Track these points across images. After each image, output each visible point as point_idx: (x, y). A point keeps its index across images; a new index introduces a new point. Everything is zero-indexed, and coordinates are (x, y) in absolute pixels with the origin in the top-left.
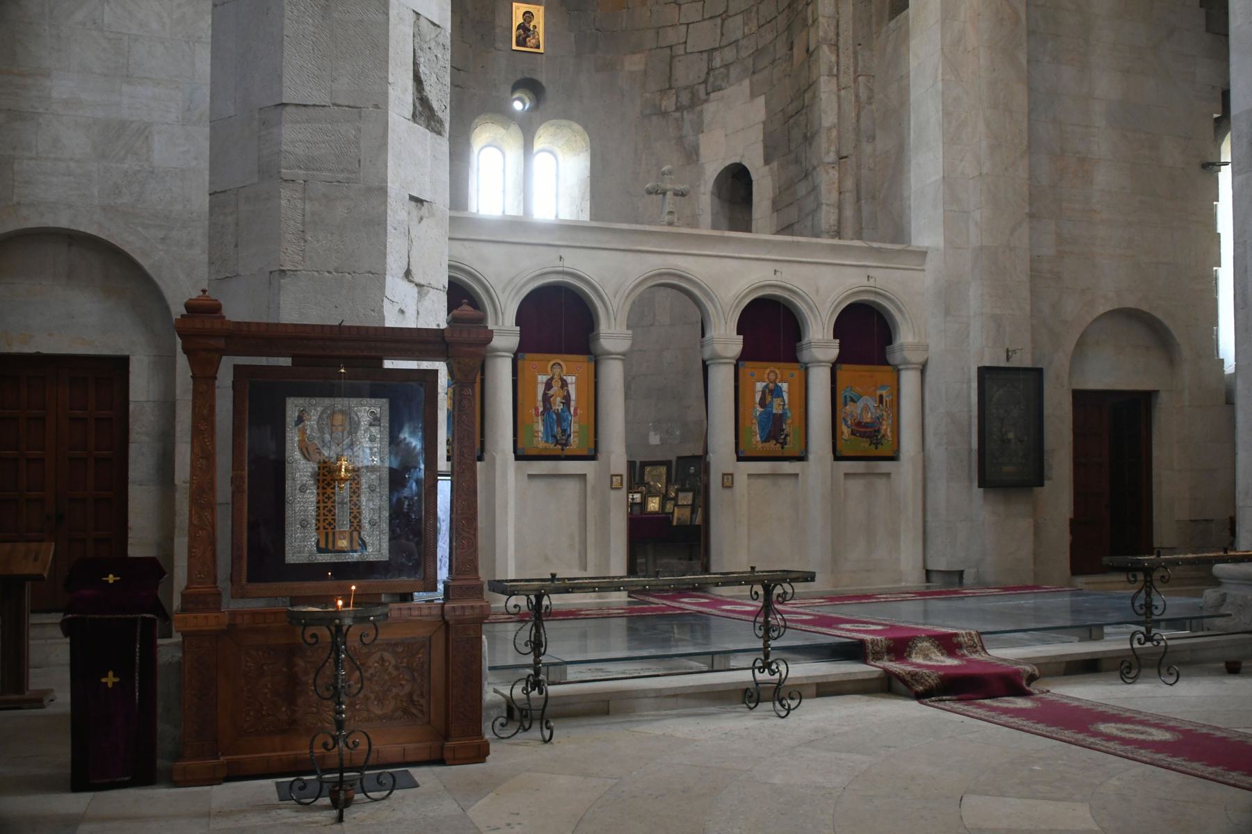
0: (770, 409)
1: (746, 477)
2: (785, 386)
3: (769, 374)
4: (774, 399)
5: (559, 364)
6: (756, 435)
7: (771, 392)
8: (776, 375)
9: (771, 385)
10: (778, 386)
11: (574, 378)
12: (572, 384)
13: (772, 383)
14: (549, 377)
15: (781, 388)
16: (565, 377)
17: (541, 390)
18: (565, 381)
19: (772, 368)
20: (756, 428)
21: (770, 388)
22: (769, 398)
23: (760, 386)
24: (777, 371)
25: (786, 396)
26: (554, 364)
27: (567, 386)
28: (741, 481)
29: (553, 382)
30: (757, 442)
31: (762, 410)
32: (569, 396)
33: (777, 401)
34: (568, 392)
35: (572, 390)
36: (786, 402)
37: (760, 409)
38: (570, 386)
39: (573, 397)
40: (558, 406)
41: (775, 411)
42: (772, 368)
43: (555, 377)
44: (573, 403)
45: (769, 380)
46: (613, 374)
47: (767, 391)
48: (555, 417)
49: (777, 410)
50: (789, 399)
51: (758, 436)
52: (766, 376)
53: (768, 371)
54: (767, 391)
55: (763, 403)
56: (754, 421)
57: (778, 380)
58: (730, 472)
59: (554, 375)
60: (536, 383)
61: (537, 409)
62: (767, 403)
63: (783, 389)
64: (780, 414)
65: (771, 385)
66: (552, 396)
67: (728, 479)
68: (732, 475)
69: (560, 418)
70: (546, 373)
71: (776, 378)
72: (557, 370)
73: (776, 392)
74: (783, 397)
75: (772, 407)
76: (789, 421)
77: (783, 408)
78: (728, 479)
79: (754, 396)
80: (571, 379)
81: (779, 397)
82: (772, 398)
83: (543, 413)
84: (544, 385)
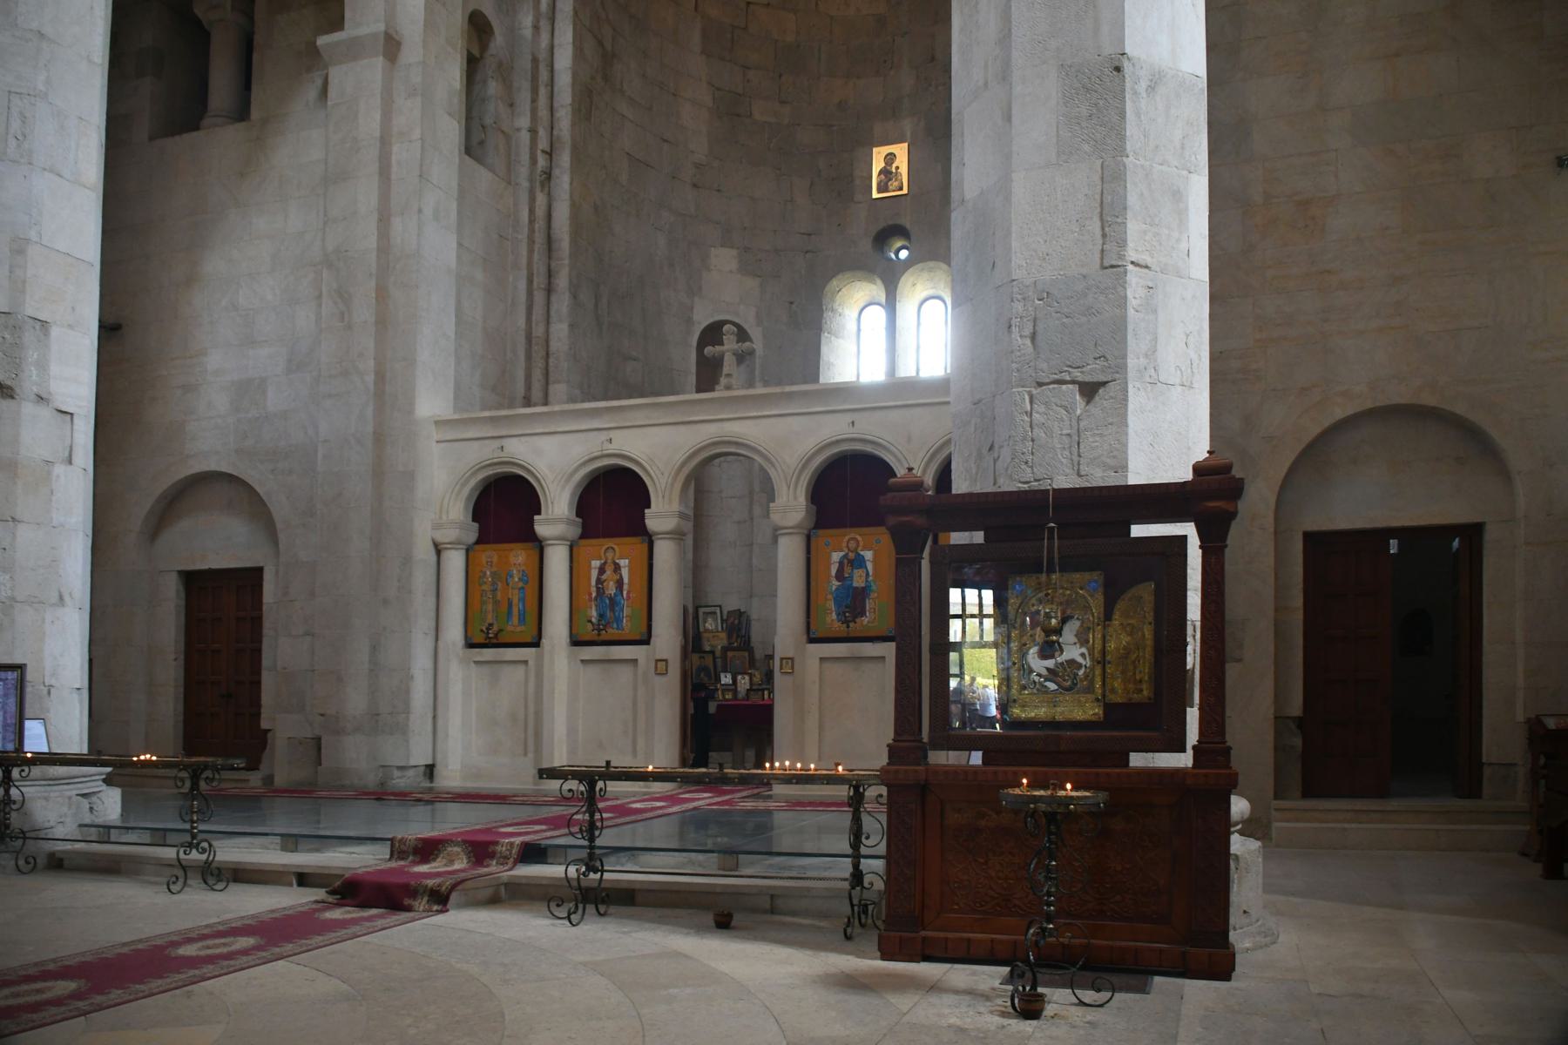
0: (849, 582)
1: (818, 661)
2: (868, 555)
3: (848, 542)
4: (855, 571)
5: (612, 548)
7: (851, 562)
8: (858, 542)
9: (852, 555)
10: (859, 554)
11: (627, 561)
12: (625, 567)
13: (852, 552)
14: (603, 562)
16: (617, 561)
17: (594, 574)
18: (618, 564)
19: (852, 535)
22: (847, 570)
23: (836, 557)
24: (859, 538)
25: (870, 566)
26: (608, 548)
27: (620, 570)
28: (812, 665)
29: (606, 567)
30: (833, 620)
31: (840, 583)
32: (622, 580)
35: (625, 573)
36: (871, 574)
37: (835, 583)
38: (623, 570)
39: (626, 580)
40: (611, 589)
41: (855, 584)
42: (852, 535)
43: (609, 561)
44: (626, 587)
46: (665, 554)
47: (846, 561)
48: (607, 601)
49: (858, 581)
50: (875, 569)
51: (834, 614)
52: (844, 545)
53: (847, 538)
55: (840, 576)
57: (860, 549)
58: (790, 655)
61: (590, 594)
63: (866, 559)
64: (863, 588)
65: (850, 554)
66: (605, 580)
67: (787, 663)
68: (792, 659)
69: (613, 603)
71: (858, 546)
72: (610, 555)
73: (858, 562)
74: (866, 568)
75: (852, 580)
76: (874, 595)
77: (867, 581)
78: (787, 663)
79: (829, 569)
80: (624, 563)
83: (596, 599)
84: (597, 570)
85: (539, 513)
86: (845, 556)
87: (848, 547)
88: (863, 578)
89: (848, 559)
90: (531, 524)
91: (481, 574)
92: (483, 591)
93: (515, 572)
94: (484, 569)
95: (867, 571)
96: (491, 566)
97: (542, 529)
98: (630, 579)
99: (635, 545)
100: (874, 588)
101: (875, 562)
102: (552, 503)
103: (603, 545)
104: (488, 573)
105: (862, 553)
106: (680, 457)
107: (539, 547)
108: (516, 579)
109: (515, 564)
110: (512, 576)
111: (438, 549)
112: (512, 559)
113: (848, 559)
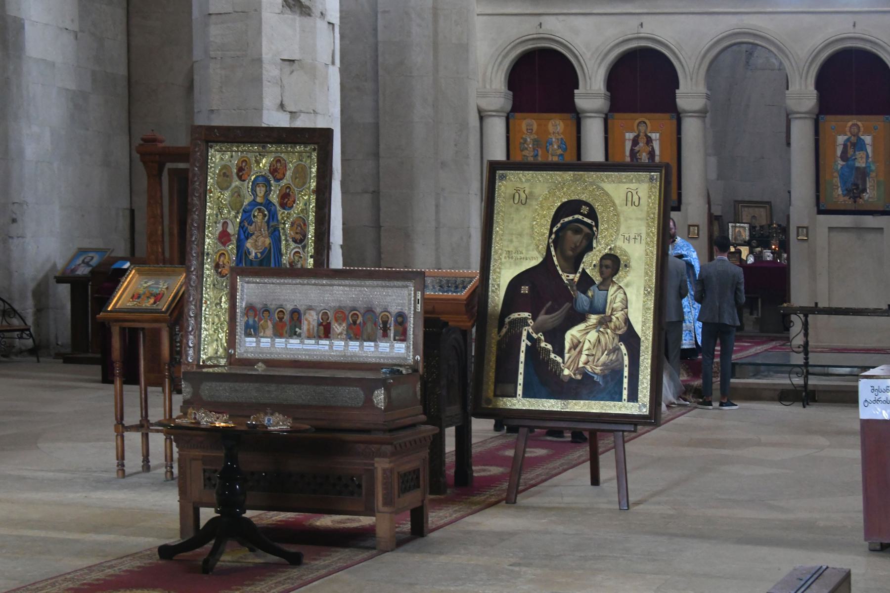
2: (868, 139)
3: (850, 127)
4: (857, 153)
5: (645, 123)
6: (837, 189)
7: (854, 145)
8: (859, 127)
9: (853, 139)
10: (861, 139)
11: (658, 135)
12: (656, 140)
13: (854, 136)
14: (636, 134)
15: (863, 141)
16: (649, 134)
17: (628, 146)
18: (650, 137)
20: (837, 181)
21: (852, 141)
22: (850, 152)
23: (841, 139)
25: (869, 149)
27: (652, 142)
29: (640, 140)
31: (844, 163)
33: (860, 154)
34: (653, 148)
35: (656, 146)
38: (654, 142)
39: (657, 152)
41: (857, 165)
42: (855, 122)
43: (641, 134)
45: (851, 133)
46: (692, 129)
47: (849, 144)
50: (874, 151)
52: (847, 129)
54: (849, 144)
55: (844, 157)
56: (836, 174)
57: (861, 133)
59: (639, 132)
60: (623, 140)
62: (849, 156)
66: (639, 151)
70: (632, 131)
71: (859, 131)
72: (642, 128)
73: (858, 145)
74: (866, 150)
76: (873, 174)
77: (867, 162)
80: (655, 136)
81: (862, 150)
82: (855, 152)
84: (631, 142)
85: (577, 88)
86: (848, 140)
87: (850, 131)
88: (864, 160)
89: (851, 142)
90: (572, 96)
91: (522, 141)
92: (525, 156)
93: (554, 140)
94: (524, 136)
95: (867, 152)
96: (531, 133)
97: (581, 102)
98: (661, 151)
99: (666, 121)
100: (873, 168)
101: (874, 144)
102: (590, 79)
103: (636, 120)
104: (529, 140)
105: (862, 137)
106: (706, 43)
107: (577, 118)
108: (555, 147)
109: (554, 133)
110: (551, 144)
111: (482, 117)
112: (551, 128)
113: (851, 142)
